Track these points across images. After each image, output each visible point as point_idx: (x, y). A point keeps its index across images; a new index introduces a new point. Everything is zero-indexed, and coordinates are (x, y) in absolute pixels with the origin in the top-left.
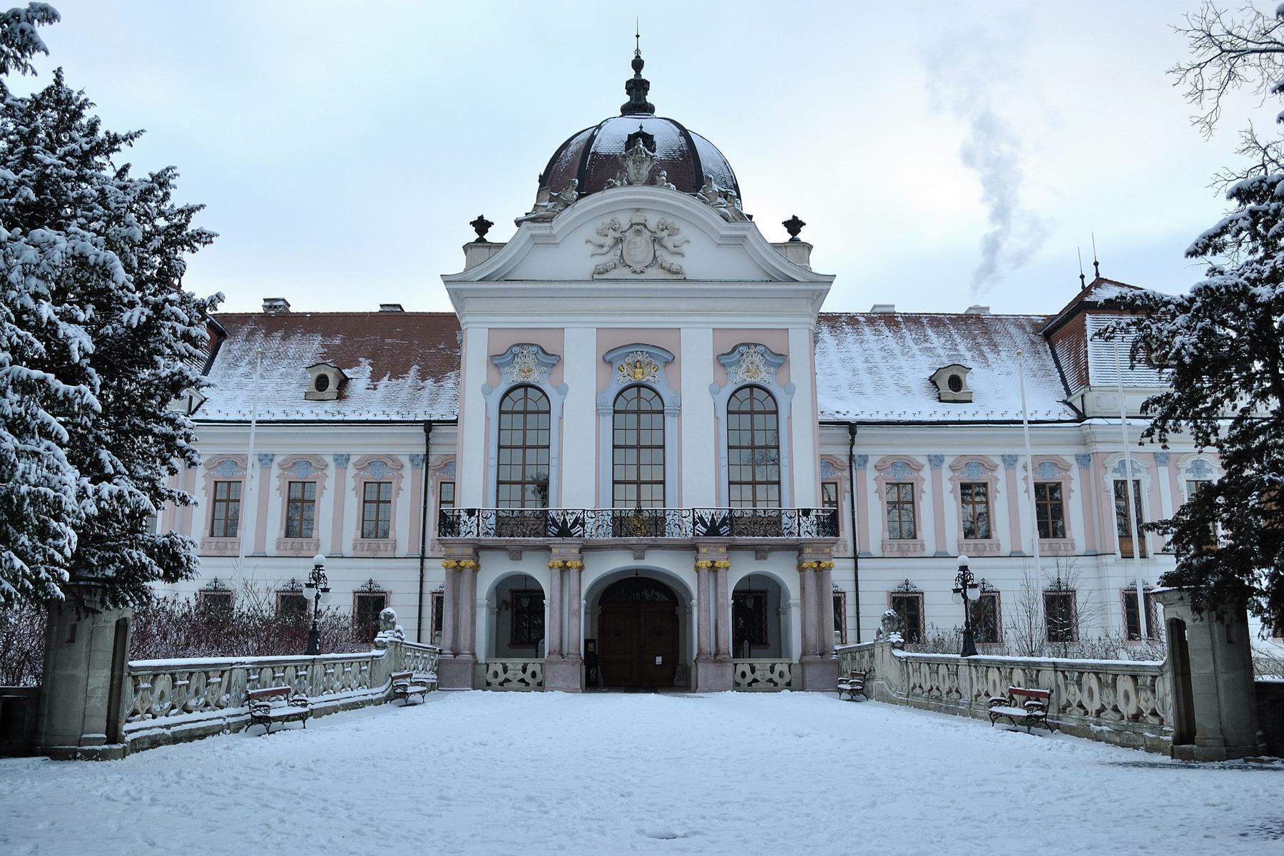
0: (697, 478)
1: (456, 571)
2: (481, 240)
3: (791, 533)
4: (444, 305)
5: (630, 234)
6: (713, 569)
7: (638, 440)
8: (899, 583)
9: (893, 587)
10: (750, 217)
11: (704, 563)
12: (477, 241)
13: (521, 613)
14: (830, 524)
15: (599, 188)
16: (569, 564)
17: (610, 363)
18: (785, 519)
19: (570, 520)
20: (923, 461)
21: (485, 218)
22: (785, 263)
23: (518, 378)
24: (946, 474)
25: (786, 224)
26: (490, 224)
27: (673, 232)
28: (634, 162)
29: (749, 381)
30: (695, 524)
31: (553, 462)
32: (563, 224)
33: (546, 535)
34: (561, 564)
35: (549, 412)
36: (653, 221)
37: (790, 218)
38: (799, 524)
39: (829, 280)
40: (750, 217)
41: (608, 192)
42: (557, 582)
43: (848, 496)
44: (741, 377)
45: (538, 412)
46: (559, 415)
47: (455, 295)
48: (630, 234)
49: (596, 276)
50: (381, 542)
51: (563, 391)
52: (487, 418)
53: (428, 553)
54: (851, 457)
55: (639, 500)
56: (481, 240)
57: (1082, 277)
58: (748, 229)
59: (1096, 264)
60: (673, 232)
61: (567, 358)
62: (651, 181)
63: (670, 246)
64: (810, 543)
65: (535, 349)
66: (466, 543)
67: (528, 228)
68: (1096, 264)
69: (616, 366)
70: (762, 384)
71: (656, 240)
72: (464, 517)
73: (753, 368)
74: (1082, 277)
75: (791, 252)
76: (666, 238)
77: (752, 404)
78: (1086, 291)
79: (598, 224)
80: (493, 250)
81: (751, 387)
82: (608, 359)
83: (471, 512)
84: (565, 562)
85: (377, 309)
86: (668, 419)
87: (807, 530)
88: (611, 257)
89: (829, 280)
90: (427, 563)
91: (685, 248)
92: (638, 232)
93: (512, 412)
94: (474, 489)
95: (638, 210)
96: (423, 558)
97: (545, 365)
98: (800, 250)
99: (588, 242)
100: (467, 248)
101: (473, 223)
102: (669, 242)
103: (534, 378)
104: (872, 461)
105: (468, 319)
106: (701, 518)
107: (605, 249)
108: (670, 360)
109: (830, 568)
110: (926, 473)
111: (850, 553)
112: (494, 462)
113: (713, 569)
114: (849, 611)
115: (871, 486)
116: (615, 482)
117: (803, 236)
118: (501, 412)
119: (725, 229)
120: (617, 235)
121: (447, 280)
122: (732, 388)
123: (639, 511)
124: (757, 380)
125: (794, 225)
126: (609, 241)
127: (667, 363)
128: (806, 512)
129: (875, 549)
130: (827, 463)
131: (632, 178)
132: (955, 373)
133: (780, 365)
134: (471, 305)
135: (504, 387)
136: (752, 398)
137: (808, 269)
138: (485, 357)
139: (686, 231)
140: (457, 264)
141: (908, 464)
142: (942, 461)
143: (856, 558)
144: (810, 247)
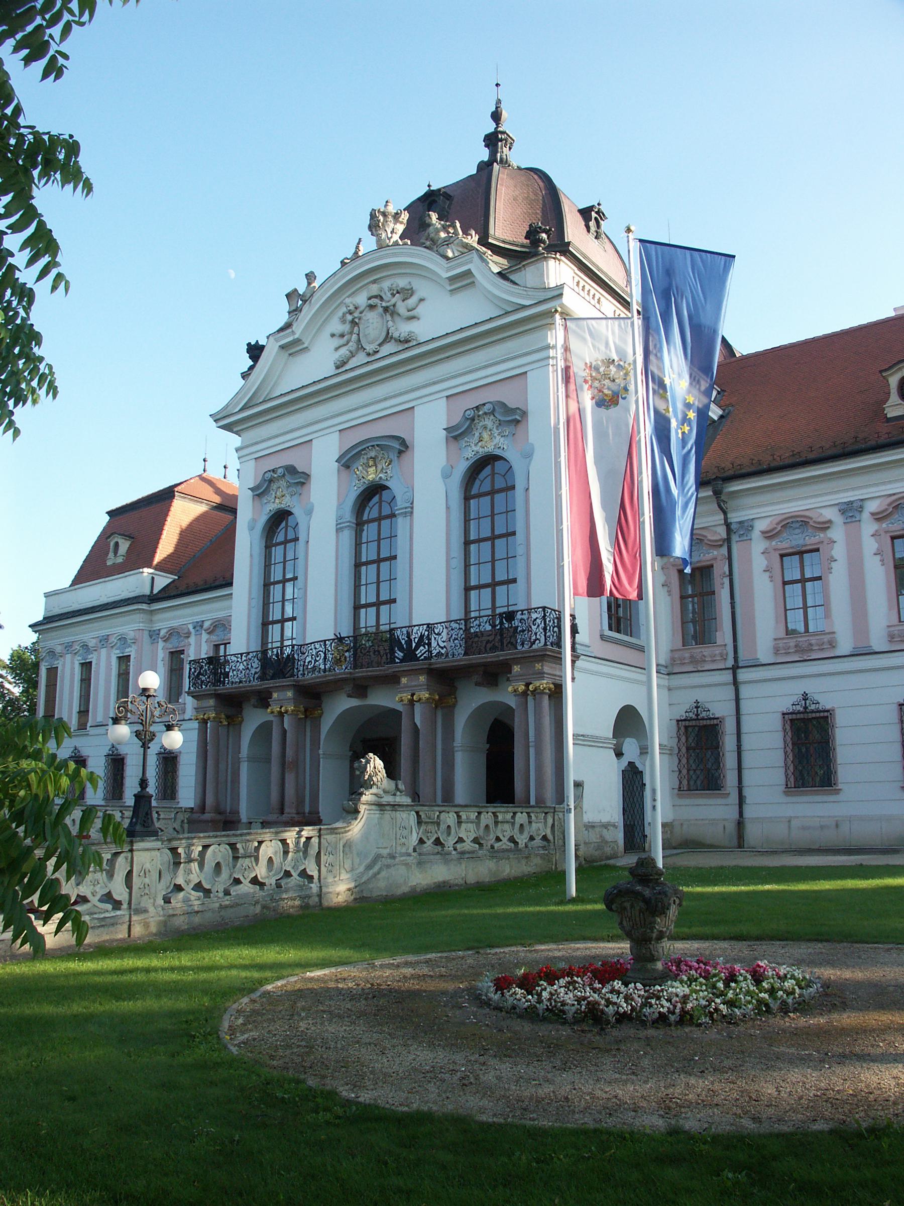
8: (794, 699)
27: (407, 293)
44: (472, 450)
60: (407, 293)
61: (315, 472)
73: (486, 436)
79: (340, 314)
88: (352, 346)
91: (420, 310)
92: (372, 307)
99: (333, 335)
102: (402, 308)
108: (402, 447)
110: (837, 533)
111: (730, 662)
119: (448, 270)
127: (400, 452)
129: (764, 653)
139: (422, 288)
143: (735, 669)
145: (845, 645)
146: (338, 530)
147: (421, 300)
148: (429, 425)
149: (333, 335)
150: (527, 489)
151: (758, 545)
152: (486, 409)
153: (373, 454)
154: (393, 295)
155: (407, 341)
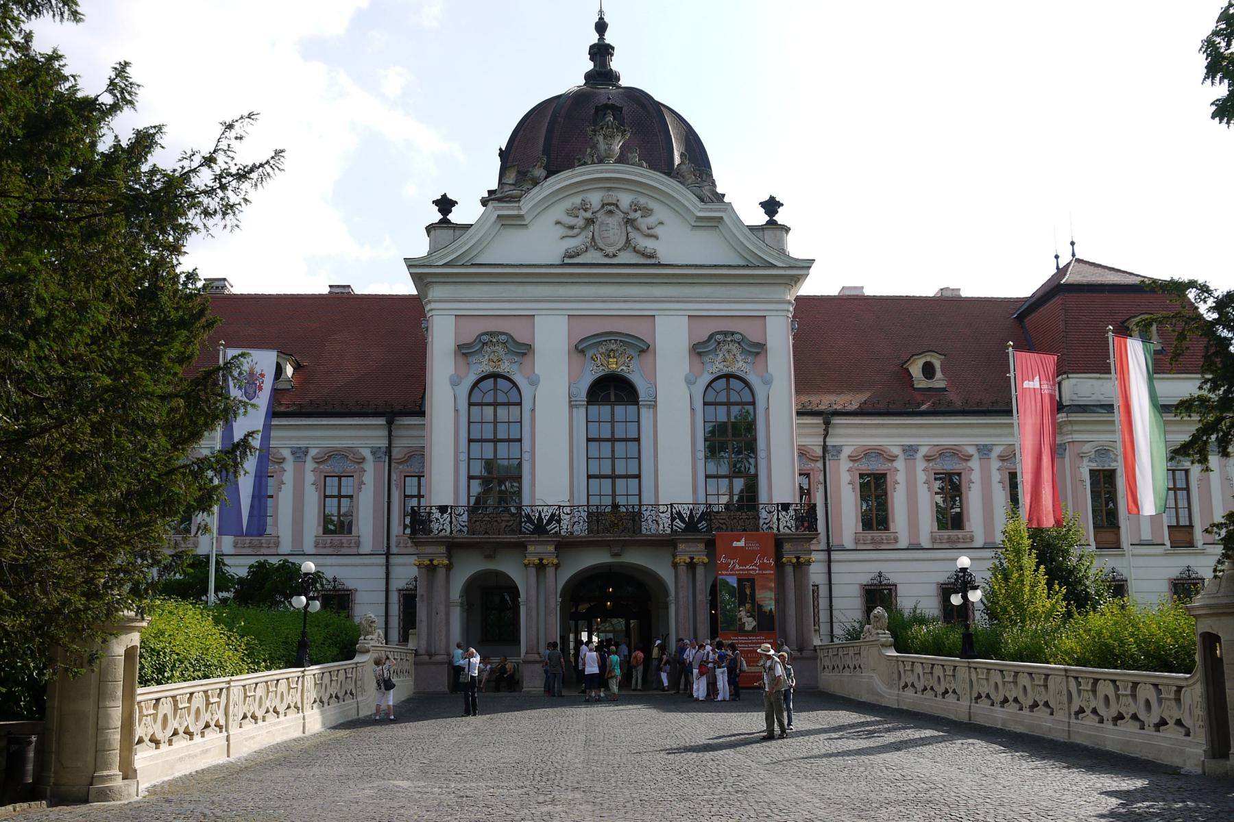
0: (675, 472)
1: (431, 569)
2: (445, 222)
3: (770, 528)
4: (406, 287)
5: (601, 216)
6: (692, 566)
7: (613, 433)
9: (866, 579)
10: (723, 195)
11: (683, 558)
12: (441, 221)
13: (493, 612)
14: (807, 518)
15: (570, 166)
16: (545, 561)
17: (582, 352)
18: (763, 514)
19: (546, 517)
20: (896, 451)
21: (450, 196)
22: (763, 246)
23: (489, 369)
24: (921, 465)
25: (763, 205)
26: (454, 203)
27: (647, 212)
28: (605, 137)
29: (725, 370)
30: (673, 519)
31: (526, 456)
32: (530, 205)
33: (521, 532)
34: (537, 561)
35: (520, 404)
36: (625, 200)
37: (767, 198)
38: (778, 519)
39: (807, 265)
40: (723, 195)
41: (579, 170)
42: (533, 579)
43: (821, 488)
44: (717, 366)
45: (509, 404)
46: (531, 406)
47: (417, 279)
48: (601, 216)
49: (567, 261)
50: (344, 538)
51: (534, 382)
52: (456, 410)
53: (394, 550)
54: (825, 447)
55: (614, 495)
56: (445, 222)
57: (1057, 257)
58: (724, 211)
59: (1073, 244)
60: (647, 212)
61: (538, 346)
62: (622, 159)
63: (644, 228)
64: (789, 539)
65: (503, 337)
66: (438, 542)
67: (496, 208)
68: (1073, 244)
69: (590, 353)
70: (739, 373)
71: (629, 222)
72: (436, 514)
74: (1057, 257)
75: (768, 235)
76: (640, 220)
77: (728, 396)
78: (1061, 272)
79: (567, 204)
80: (458, 232)
81: (728, 376)
82: (580, 349)
83: (443, 509)
84: (541, 560)
85: (326, 291)
86: (644, 411)
87: (786, 523)
89: (807, 265)
90: (393, 560)
91: (659, 231)
92: (610, 212)
93: (482, 404)
94: (446, 484)
95: (609, 189)
96: (388, 554)
97: (517, 354)
98: (778, 232)
99: (558, 223)
100: (430, 229)
101: (436, 202)
102: (643, 223)
103: (504, 368)
104: (847, 451)
105: (433, 305)
106: (679, 514)
107: (576, 231)
108: (644, 348)
109: (809, 563)
110: (900, 464)
111: (823, 546)
112: (464, 457)
113: (692, 566)
114: (823, 603)
115: (845, 477)
116: (589, 477)
117: (780, 218)
118: (470, 404)
120: (588, 215)
121: (411, 263)
122: (709, 378)
123: (615, 506)
124: (733, 370)
125: (771, 206)
126: (580, 222)
127: (642, 351)
128: (786, 507)
129: (848, 544)
130: (803, 453)
131: (603, 153)
132: (928, 359)
133: (758, 353)
134: (436, 292)
135: (472, 378)
136: (728, 388)
137: (782, 252)
138: (451, 346)
139: (660, 212)
140: (420, 247)
141: (878, 453)
142: (916, 451)
143: (829, 550)
144: (787, 230)
145: (903, 542)
146: (572, 406)
147: (661, 223)
148: (672, 337)
149: (558, 223)
150: (767, 409)
151: (845, 465)
152: (737, 337)
153: (614, 347)
154: (636, 211)
155: (651, 256)
